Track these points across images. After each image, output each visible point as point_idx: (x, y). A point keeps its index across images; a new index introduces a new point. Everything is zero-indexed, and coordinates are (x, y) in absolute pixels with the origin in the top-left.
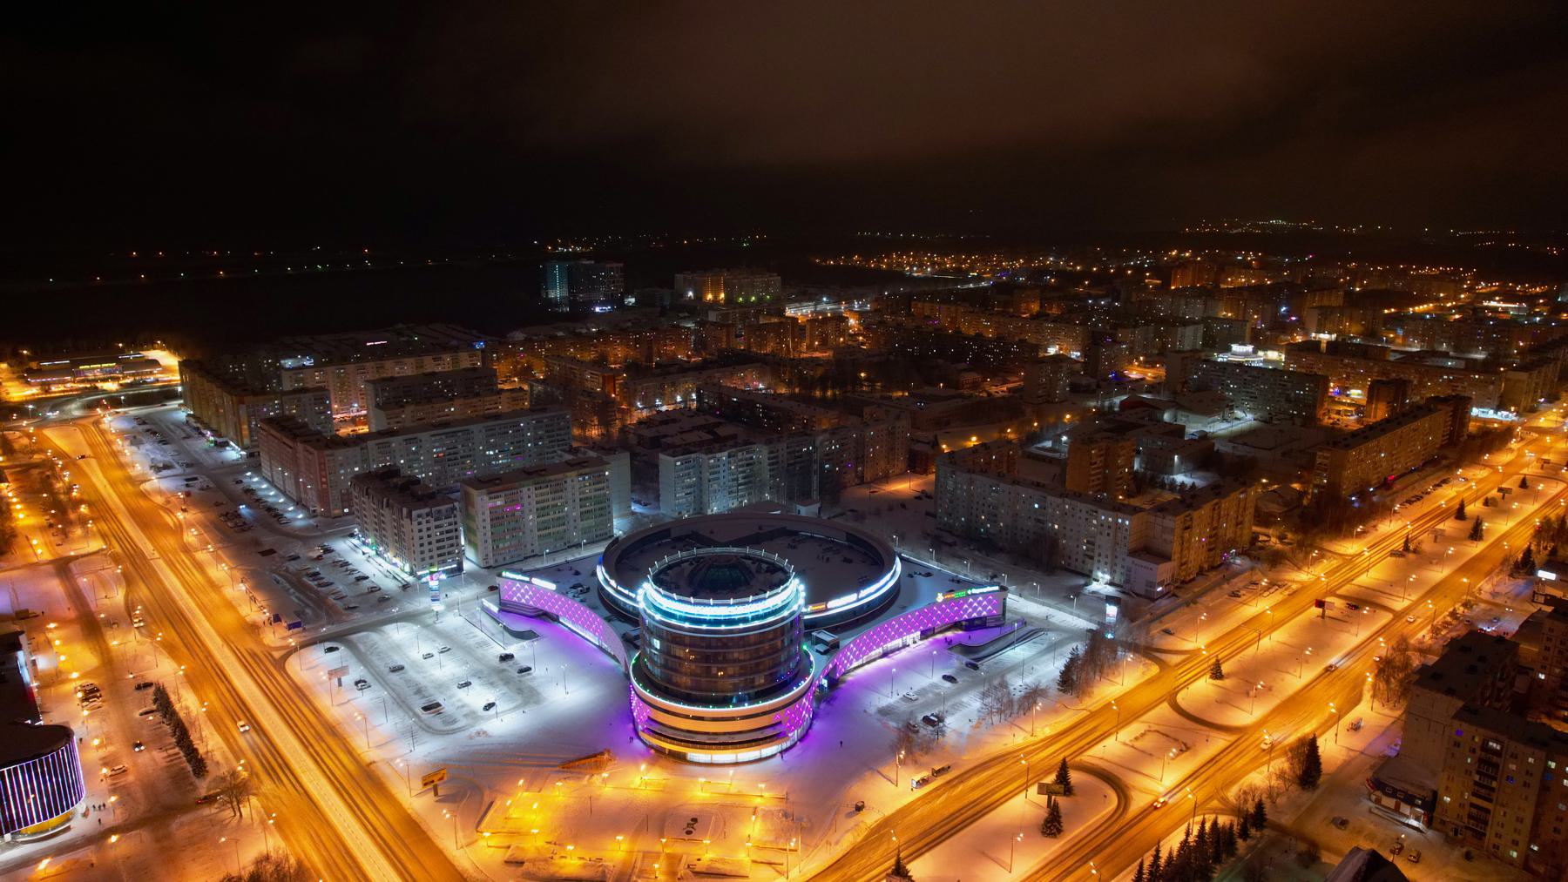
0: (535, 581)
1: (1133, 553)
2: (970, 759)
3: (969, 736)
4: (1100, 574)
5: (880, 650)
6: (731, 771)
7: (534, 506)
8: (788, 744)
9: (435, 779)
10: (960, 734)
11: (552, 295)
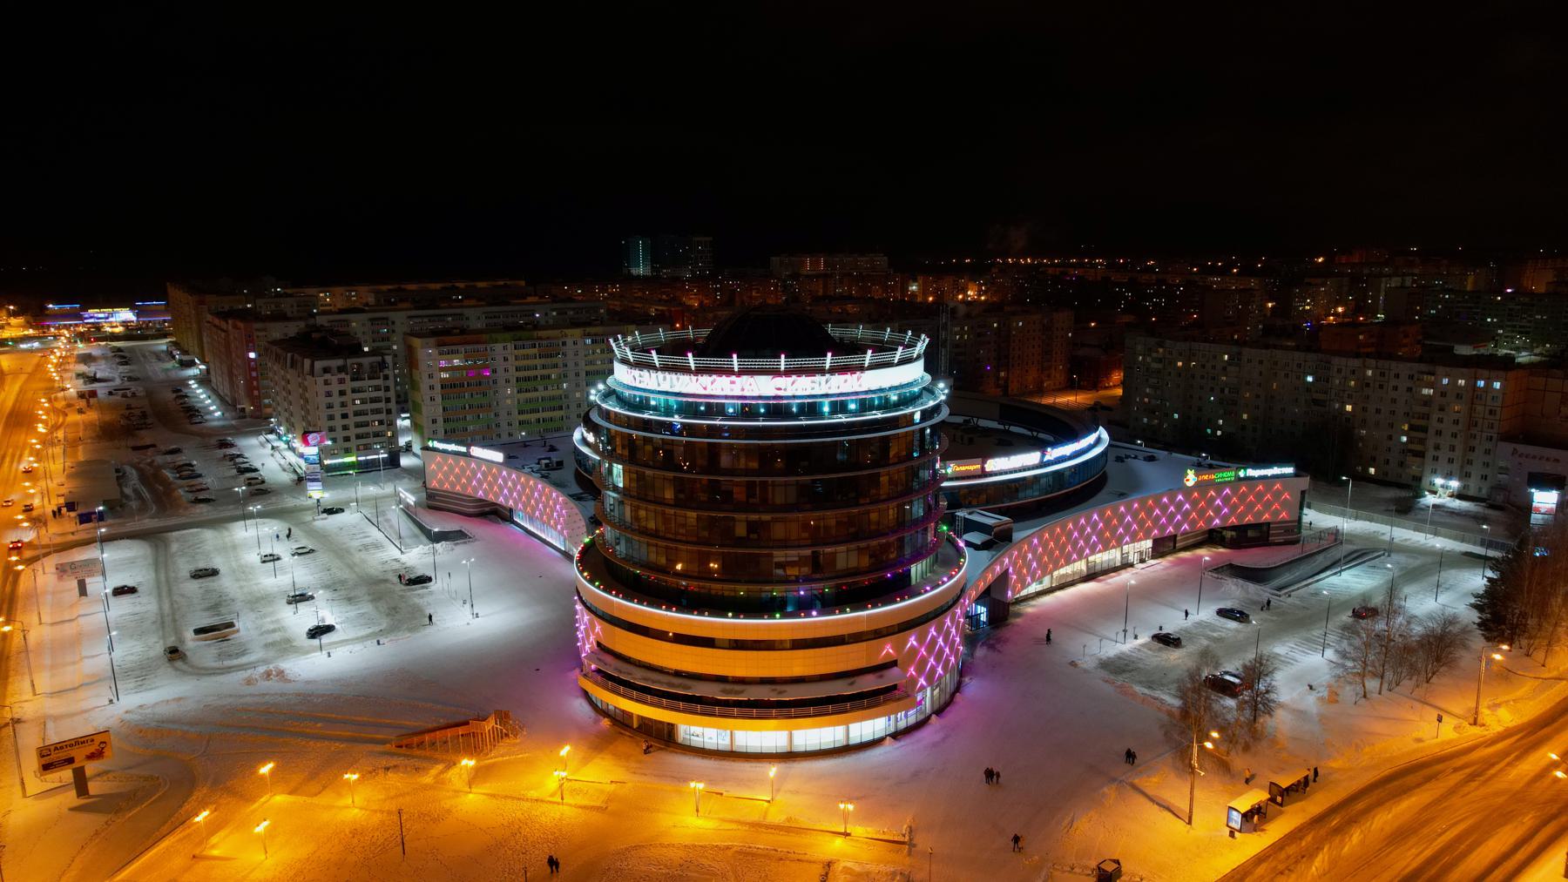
0: (476, 451)
1: (1507, 437)
2: (1348, 770)
3: (1323, 719)
4: (1439, 481)
5: (1080, 566)
6: (773, 770)
7: (513, 374)
8: (913, 717)
9: (79, 754)
10: (1300, 714)
11: (634, 271)
